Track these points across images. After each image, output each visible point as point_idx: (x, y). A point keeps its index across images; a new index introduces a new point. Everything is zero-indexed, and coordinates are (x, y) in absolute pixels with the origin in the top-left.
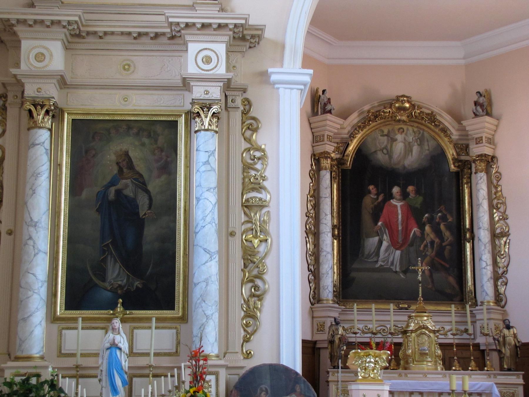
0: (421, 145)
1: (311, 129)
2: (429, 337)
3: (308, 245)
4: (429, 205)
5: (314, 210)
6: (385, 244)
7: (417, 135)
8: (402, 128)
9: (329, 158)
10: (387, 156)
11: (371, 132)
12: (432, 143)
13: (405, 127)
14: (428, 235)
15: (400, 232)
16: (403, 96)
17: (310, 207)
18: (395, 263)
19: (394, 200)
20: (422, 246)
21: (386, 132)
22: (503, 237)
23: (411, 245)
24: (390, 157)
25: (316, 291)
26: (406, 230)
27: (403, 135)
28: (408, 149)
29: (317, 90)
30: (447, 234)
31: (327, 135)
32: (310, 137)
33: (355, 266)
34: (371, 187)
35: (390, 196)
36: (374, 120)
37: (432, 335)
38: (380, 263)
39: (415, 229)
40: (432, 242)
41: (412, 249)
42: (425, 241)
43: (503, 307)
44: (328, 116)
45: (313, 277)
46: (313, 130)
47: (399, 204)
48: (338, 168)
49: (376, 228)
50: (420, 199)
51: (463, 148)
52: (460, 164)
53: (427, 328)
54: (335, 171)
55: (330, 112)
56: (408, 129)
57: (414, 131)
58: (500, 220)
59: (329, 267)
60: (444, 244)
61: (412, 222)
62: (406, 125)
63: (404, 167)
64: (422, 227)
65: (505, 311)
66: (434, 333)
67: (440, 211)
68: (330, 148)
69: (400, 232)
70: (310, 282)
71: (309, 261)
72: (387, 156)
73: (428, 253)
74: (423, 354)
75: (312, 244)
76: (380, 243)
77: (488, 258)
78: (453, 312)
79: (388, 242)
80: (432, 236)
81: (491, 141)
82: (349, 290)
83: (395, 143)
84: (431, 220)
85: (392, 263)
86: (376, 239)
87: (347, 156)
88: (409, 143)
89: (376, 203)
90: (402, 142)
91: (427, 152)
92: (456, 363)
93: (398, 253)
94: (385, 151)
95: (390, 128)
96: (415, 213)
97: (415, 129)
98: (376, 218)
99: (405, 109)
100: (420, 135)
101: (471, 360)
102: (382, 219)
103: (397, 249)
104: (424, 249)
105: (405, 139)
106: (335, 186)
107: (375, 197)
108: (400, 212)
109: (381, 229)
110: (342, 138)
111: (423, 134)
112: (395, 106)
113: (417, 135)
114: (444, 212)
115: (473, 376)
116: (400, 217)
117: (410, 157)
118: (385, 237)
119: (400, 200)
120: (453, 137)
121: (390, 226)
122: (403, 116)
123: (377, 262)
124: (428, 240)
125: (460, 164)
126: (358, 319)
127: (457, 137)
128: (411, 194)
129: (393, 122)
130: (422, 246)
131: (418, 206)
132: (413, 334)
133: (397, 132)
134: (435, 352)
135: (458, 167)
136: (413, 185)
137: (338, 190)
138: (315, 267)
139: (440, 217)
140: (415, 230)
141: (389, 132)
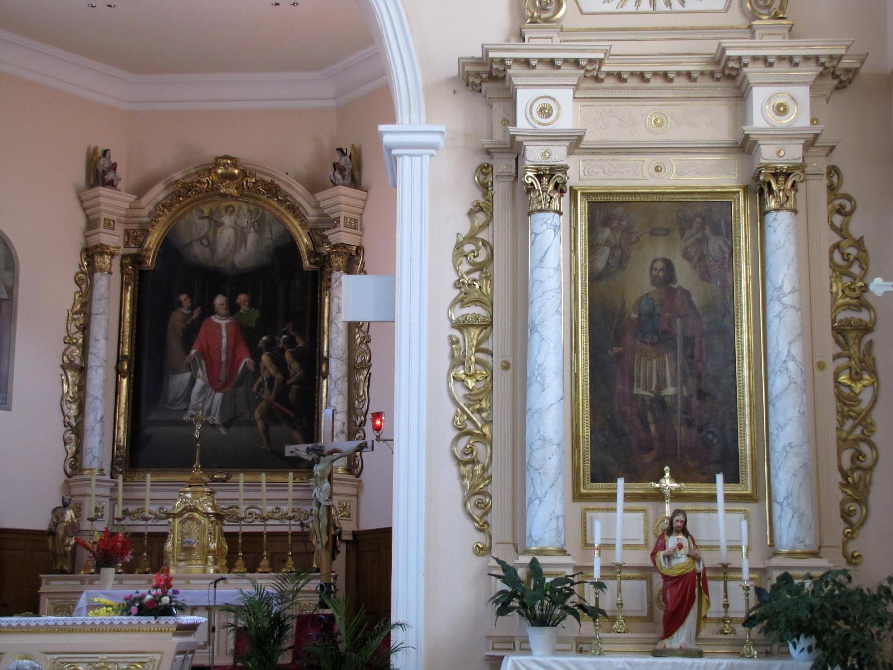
0: (259, 231)
1: (84, 210)
2: (199, 522)
3: (66, 387)
4: (268, 324)
5: (83, 333)
6: (200, 383)
7: (254, 216)
8: (231, 206)
9: (107, 253)
10: (208, 250)
11: (184, 213)
12: (276, 229)
13: (236, 205)
14: (265, 368)
15: (224, 365)
16: (226, 157)
17: (74, 329)
18: (213, 411)
19: (217, 316)
20: (255, 386)
21: (207, 212)
22: (363, 369)
23: (239, 383)
24: (213, 251)
25: (78, 456)
26: (233, 362)
27: (233, 217)
28: (240, 236)
29: (95, 150)
30: (294, 367)
31: (105, 219)
32: (82, 222)
33: (153, 417)
34: (183, 297)
35: (212, 311)
36: (186, 196)
37: (204, 521)
38: (190, 412)
39: (247, 360)
40: (271, 379)
41: (240, 390)
43: (358, 476)
44: (102, 190)
45: (73, 436)
46: (88, 212)
47: (223, 322)
48: (135, 268)
49: (187, 359)
50: (256, 314)
51: (317, 234)
52: (318, 259)
53: (197, 510)
54: (128, 274)
55: (111, 184)
56: (240, 208)
57: (249, 210)
58: (361, 343)
59: (95, 419)
60: (288, 382)
61: (242, 348)
62: (237, 200)
63: (233, 265)
64: (256, 356)
65: (360, 482)
66: (209, 518)
67: (285, 332)
68: (112, 239)
69: (224, 365)
70: (66, 443)
71: (66, 412)
72: (208, 250)
73: (264, 396)
74: (187, 550)
75: (75, 384)
76: (193, 381)
77: (340, 401)
78: (291, 484)
79: (204, 380)
80: (272, 370)
81: (356, 225)
82: (138, 454)
83: (220, 230)
84: (270, 346)
85: (209, 413)
86: (187, 375)
87: (147, 250)
88: (242, 228)
89: (189, 322)
90: (231, 227)
91: (269, 241)
92: (265, 562)
93: (219, 396)
94: (205, 242)
95: (213, 206)
96: (247, 336)
97: (252, 208)
98: (188, 345)
99: (232, 177)
100: (259, 216)
101: (262, 557)
102: (197, 345)
103: (217, 390)
104: (258, 389)
105: (235, 223)
106: (128, 296)
107: (189, 312)
108: (224, 334)
109: (194, 360)
110: (141, 223)
111: (263, 216)
112: (216, 173)
113: (254, 216)
114: (292, 333)
115: (125, 582)
116: (224, 341)
117: (243, 250)
118: (200, 372)
119: (226, 316)
120: (309, 218)
121: (208, 356)
122: (229, 187)
123: (186, 410)
124: (265, 376)
125: (318, 259)
126: (153, 497)
127: (314, 219)
128: (242, 307)
129: (218, 198)
130: (255, 386)
131: (252, 324)
132: (177, 521)
133: (223, 212)
134: (209, 546)
135: (315, 263)
136: (245, 292)
137: (133, 302)
138: (79, 420)
139: (285, 341)
140: (246, 360)
141: (211, 212)
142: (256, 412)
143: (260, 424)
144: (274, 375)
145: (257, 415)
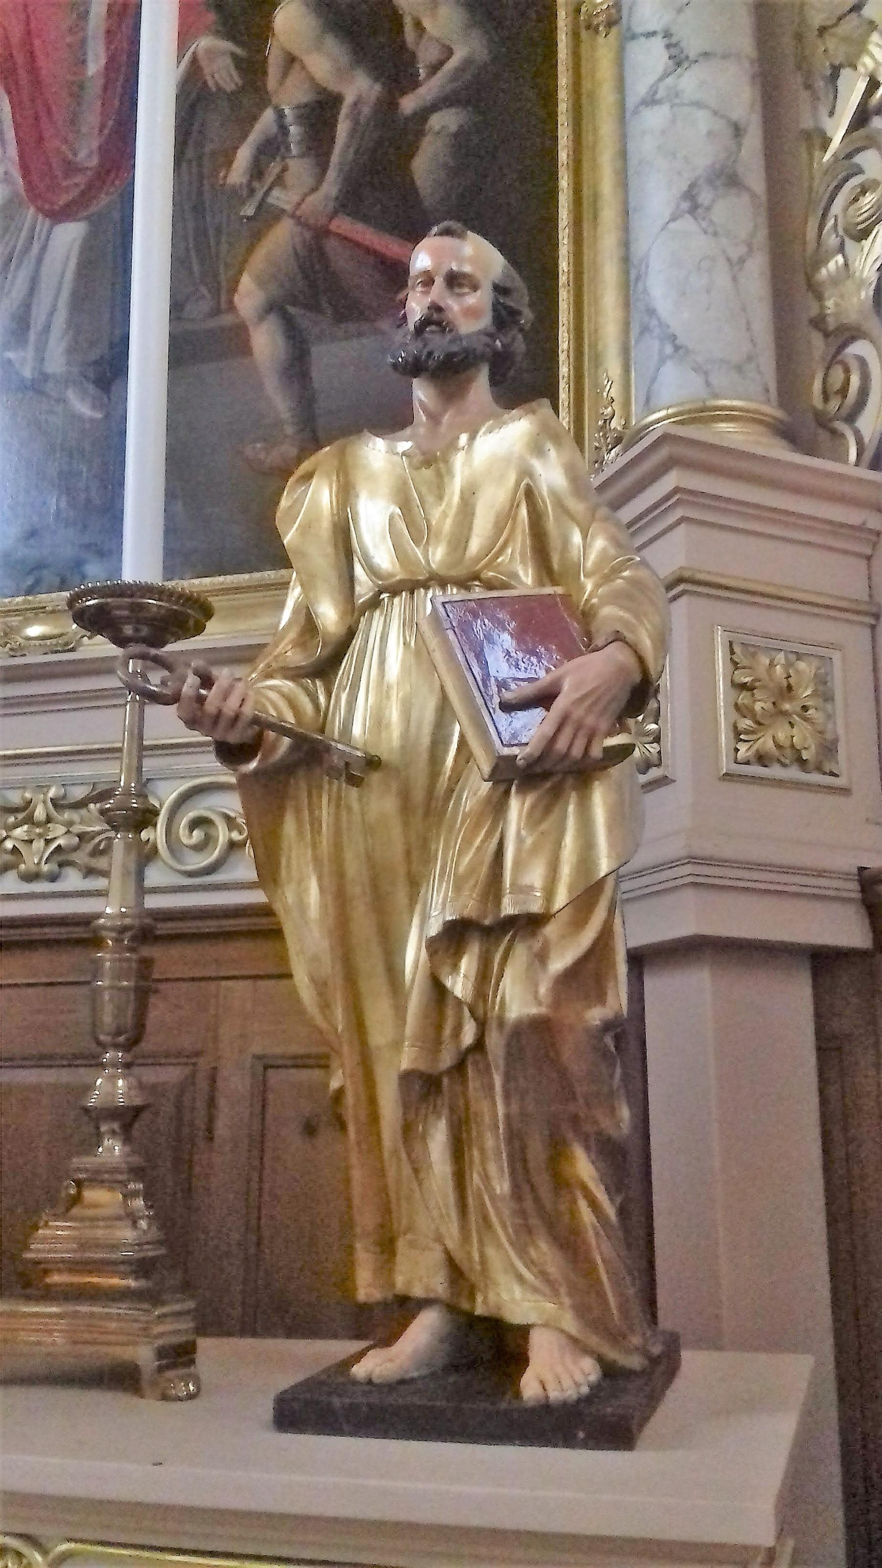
14: (291, 60)
20: (244, 155)
40: (322, 111)
42: (268, 115)
103: (59, 215)
104: (257, 171)
124: (289, 96)
130: (244, 155)
142: (246, 282)
143: (266, 342)
144: (333, 86)
145: (249, 296)
